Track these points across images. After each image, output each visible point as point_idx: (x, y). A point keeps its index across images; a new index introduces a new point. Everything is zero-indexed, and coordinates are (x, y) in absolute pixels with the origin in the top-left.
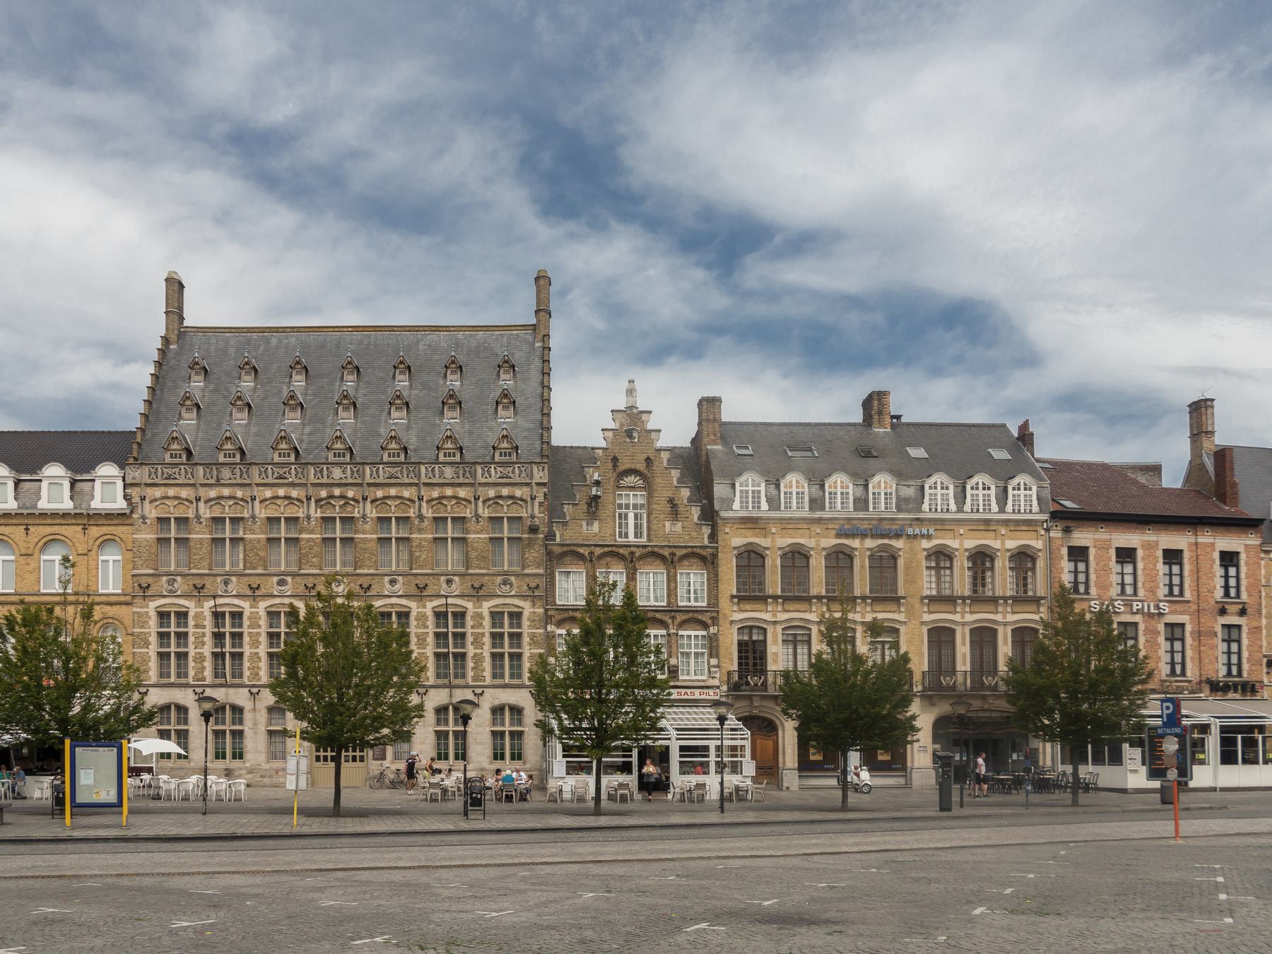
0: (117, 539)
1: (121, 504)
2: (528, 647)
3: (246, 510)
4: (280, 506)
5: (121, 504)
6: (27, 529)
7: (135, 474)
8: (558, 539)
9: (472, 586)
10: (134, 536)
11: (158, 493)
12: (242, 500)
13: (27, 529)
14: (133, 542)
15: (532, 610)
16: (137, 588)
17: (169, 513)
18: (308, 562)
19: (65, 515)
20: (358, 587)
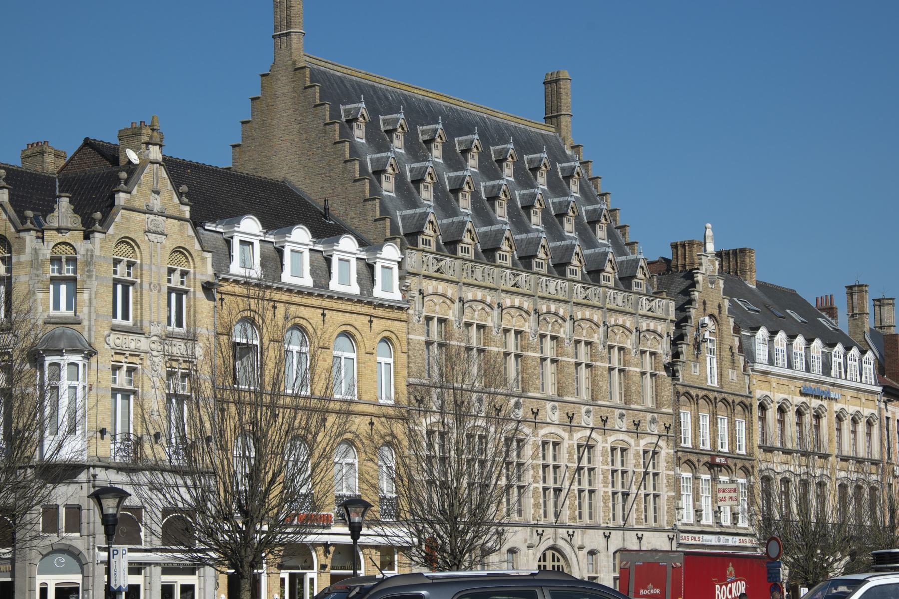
0: (393, 337)
1: (396, 295)
2: (665, 489)
3: (490, 318)
4: (513, 317)
5: (396, 295)
6: (324, 315)
7: (413, 259)
8: (681, 380)
9: (634, 421)
10: (410, 337)
11: (429, 286)
12: (489, 306)
13: (324, 315)
14: (408, 343)
15: (667, 451)
16: (413, 401)
17: (434, 312)
18: (533, 384)
19: (350, 299)
20: (566, 416)
